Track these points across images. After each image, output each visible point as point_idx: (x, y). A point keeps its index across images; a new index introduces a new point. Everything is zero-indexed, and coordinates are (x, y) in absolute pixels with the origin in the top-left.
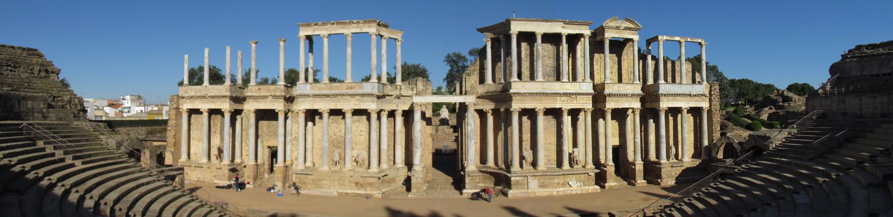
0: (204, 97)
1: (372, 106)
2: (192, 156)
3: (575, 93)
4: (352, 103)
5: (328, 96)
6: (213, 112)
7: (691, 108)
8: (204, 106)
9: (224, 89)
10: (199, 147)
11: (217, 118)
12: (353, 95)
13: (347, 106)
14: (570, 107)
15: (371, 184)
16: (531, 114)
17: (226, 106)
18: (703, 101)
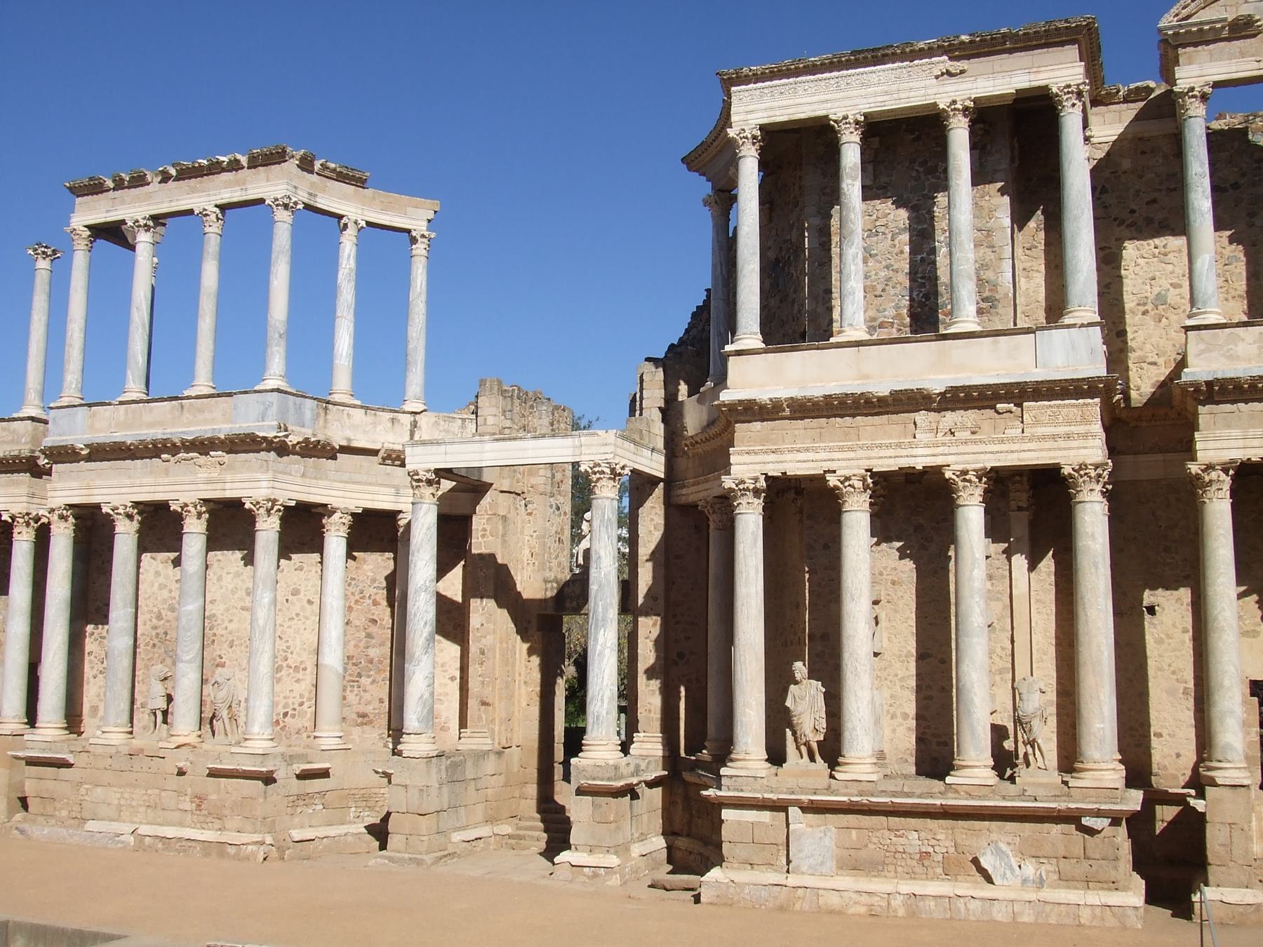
4: (202, 475)
12: (203, 446)
16: (802, 509)
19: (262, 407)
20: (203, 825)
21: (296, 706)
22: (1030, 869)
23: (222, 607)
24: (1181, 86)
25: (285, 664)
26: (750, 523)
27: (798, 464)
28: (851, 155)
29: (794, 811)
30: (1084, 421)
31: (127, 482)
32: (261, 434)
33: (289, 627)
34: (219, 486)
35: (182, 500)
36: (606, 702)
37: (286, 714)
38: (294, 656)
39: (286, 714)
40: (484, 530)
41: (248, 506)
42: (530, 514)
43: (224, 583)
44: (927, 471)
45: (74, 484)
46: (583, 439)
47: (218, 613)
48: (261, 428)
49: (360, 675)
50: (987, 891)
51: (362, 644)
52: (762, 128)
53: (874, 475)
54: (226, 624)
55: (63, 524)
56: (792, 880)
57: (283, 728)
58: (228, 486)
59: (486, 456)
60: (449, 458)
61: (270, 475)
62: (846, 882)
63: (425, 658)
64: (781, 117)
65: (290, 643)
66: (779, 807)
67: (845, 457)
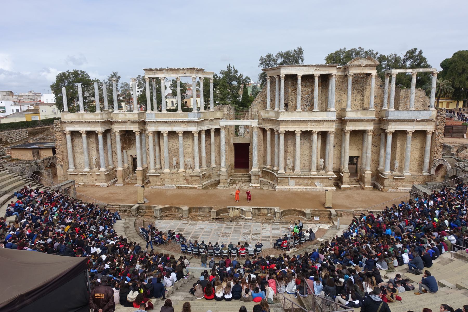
0: (82, 122)
2: (78, 166)
3: (325, 119)
5: (166, 122)
6: (89, 134)
7: (416, 131)
8: (82, 129)
9: (97, 116)
10: (82, 159)
11: (93, 140)
12: (182, 122)
13: (179, 129)
14: (319, 130)
15: (195, 180)
17: (99, 129)
18: (428, 124)
20: (189, 184)
22: (322, 185)
24: (350, 73)
26: (282, 137)
27: (290, 129)
28: (299, 81)
29: (289, 178)
30: (333, 125)
44: (310, 131)
50: (316, 188)
52: (286, 75)
53: (302, 131)
56: (289, 187)
62: (296, 187)
64: (289, 74)
66: (288, 178)
67: (298, 129)
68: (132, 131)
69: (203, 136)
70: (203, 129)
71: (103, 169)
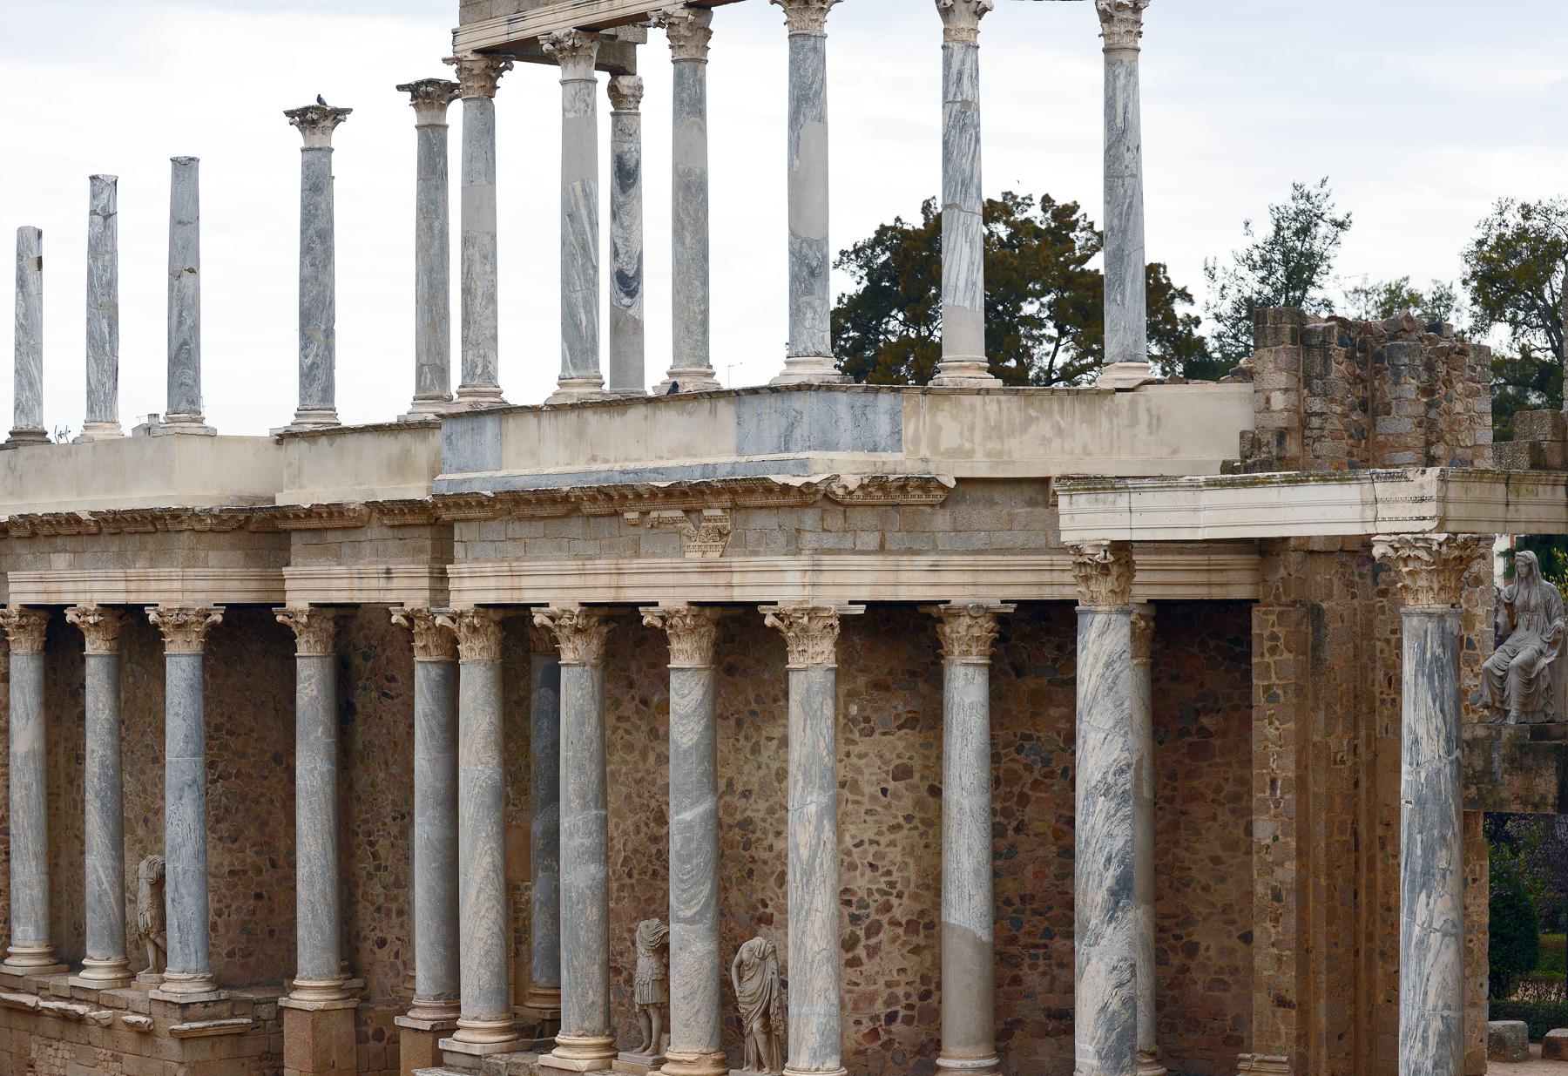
1: (778, 579)
12: (689, 496)
19: (784, 422)
21: (914, 1000)
23: (762, 806)
25: (885, 919)
31: (571, 565)
32: (780, 479)
33: (892, 844)
34: (722, 579)
35: (665, 604)
36: (1433, 1040)
37: (891, 1018)
38: (905, 900)
39: (891, 1018)
40: (1274, 637)
41: (769, 621)
42: (1383, 593)
43: (764, 758)
45: (489, 568)
46: (1379, 486)
47: (757, 817)
48: (781, 466)
49: (1048, 934)
51: (1052, 869)
54: (771, 838)
55: (478, 644)
57: (887, 1045)
58: (737, 579)
59: (1204, 518)
60: (1137, 520)
61: (805, 560)
63: (1109, 930)
65: (896, 876)
68: (384, 610)
69: (966, 690)
70: (958, 596)
71: (183, 980)
